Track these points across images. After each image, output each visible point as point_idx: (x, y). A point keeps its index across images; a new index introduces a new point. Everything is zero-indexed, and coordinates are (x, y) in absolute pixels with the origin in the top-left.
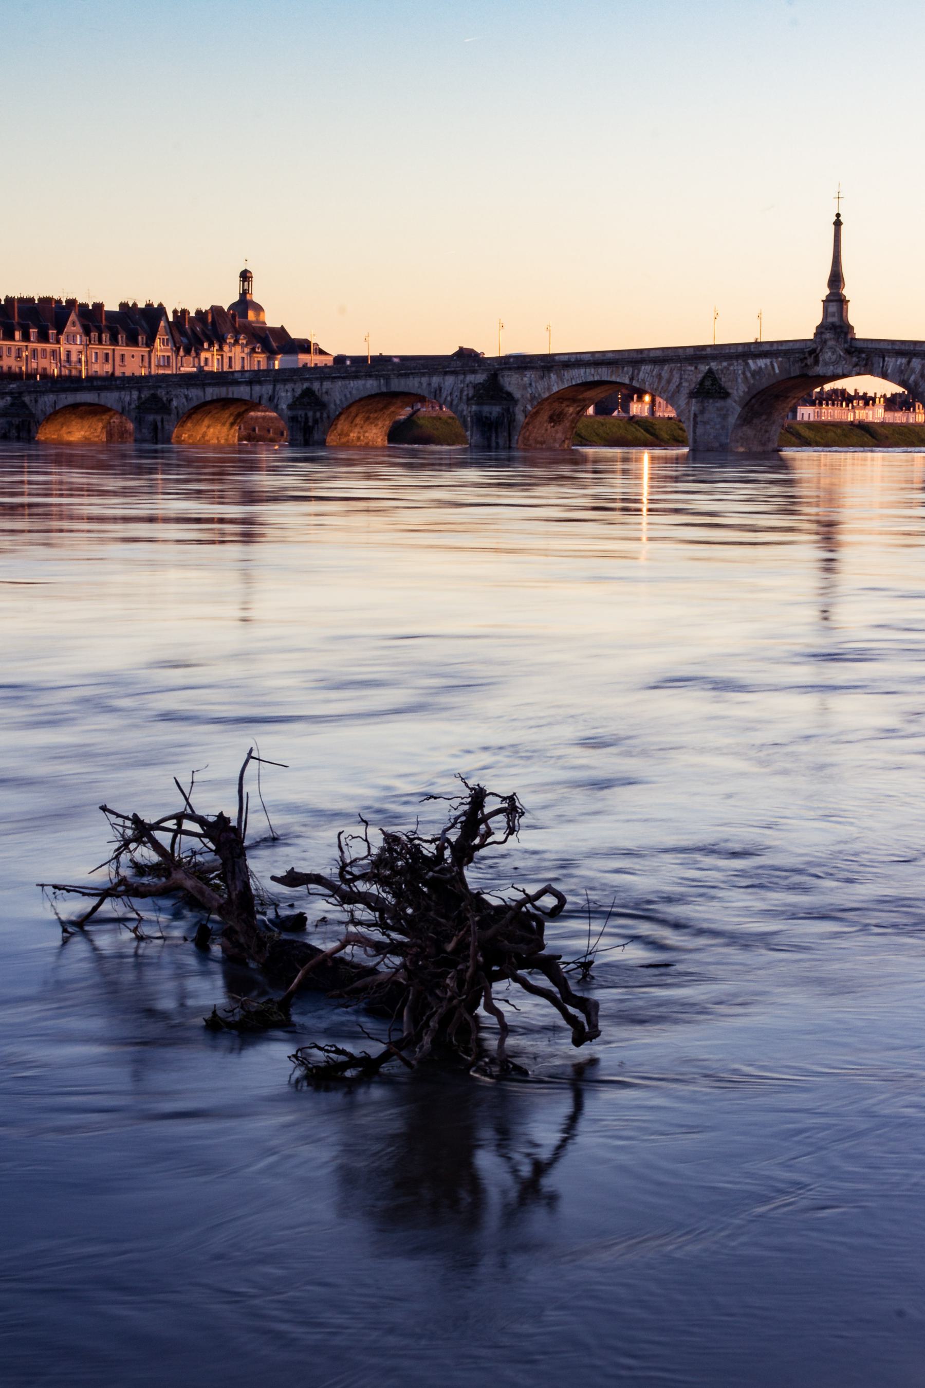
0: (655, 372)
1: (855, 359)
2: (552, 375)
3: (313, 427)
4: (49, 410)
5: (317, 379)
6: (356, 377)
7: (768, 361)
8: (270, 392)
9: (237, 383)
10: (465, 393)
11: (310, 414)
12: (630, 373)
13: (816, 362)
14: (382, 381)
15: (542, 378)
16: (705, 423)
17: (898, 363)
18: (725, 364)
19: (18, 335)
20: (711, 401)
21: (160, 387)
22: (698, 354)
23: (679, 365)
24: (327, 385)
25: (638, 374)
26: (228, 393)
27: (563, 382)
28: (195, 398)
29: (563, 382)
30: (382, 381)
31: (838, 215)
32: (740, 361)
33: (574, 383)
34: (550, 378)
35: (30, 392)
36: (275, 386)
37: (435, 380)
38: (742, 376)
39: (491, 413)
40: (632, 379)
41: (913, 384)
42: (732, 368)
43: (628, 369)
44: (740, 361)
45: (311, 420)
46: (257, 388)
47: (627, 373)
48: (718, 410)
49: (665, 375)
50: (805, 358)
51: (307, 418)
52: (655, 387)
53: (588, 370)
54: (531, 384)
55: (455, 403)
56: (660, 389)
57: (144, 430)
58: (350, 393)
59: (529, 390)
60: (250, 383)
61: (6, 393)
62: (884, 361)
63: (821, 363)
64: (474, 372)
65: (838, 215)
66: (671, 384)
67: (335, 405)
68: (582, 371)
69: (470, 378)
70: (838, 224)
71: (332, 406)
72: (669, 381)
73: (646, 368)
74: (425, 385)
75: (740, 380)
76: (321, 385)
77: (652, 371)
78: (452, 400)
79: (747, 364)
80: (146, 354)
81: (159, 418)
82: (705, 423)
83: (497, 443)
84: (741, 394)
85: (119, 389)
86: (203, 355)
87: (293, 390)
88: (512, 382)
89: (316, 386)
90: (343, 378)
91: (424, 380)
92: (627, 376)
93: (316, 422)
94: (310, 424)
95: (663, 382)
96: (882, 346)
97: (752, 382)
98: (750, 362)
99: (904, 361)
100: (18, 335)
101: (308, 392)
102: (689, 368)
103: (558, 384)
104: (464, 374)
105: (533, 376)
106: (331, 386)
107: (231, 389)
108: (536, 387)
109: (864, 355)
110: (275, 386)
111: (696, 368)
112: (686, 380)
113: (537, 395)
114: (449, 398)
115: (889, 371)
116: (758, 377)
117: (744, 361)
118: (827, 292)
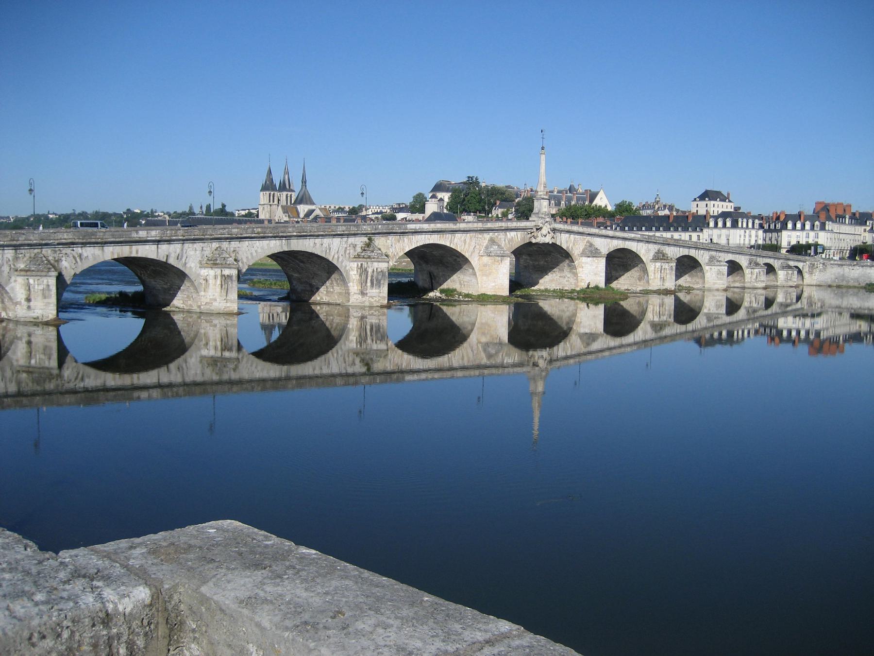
0: (462, 239)
2: (405, 239)
7: (516, 233)
8: (178, 251)
14: (284, 241)
18: (496, 234)
26: (131, 252)
27: (412, 244)
28: (90, 257)
34: (404, 241)
37: (326, 241)
43: (449, 236)
46: (164, 247)
49: (468, 241)
54: (392, 245)
66: (471, 247)
68: (423, 236)
72: (470, 245)
73: (458, 235)
74: (318, 245)
78: (338, 258)
79: (506, 235)
95: (467, 246)
99: (567, 235)
106: (239, 245)
107: (134, 248)
113: (395, 254)
114: (336, 256)
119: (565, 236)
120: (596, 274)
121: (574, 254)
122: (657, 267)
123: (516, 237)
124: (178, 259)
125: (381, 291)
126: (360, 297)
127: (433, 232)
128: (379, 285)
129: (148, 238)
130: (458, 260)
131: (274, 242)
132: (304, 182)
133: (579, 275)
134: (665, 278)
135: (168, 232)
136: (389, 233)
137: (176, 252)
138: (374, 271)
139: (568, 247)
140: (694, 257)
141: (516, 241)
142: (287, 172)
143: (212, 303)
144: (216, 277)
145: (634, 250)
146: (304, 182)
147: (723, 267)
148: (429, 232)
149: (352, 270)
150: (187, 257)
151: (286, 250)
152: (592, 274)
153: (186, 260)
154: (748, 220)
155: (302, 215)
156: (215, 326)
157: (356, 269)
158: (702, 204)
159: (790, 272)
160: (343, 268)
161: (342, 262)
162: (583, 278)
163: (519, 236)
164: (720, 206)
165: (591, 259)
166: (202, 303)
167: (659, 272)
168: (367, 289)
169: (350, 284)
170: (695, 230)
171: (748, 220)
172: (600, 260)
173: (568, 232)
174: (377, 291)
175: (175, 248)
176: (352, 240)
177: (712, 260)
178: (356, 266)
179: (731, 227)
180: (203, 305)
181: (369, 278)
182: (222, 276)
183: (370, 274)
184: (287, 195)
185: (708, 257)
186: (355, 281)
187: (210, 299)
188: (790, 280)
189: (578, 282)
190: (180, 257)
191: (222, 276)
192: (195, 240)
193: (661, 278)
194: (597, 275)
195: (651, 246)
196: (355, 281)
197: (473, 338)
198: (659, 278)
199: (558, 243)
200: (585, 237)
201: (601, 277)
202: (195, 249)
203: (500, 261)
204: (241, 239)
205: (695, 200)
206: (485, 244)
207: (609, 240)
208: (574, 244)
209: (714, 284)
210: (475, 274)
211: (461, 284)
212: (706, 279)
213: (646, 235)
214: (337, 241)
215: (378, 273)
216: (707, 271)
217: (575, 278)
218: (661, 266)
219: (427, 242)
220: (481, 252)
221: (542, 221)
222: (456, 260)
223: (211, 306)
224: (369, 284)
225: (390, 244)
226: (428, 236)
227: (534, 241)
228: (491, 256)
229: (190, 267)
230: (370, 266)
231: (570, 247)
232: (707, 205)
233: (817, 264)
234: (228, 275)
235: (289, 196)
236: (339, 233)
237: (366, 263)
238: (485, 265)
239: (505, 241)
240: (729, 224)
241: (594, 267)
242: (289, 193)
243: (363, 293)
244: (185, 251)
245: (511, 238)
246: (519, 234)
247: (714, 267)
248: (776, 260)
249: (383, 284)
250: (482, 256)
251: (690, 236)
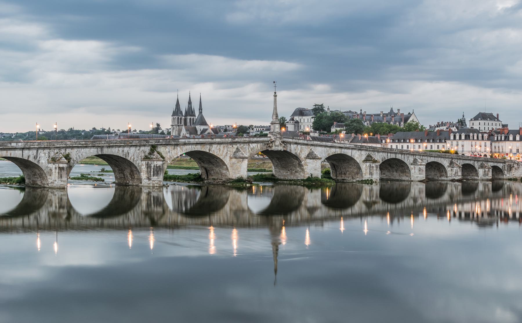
0: (218, 148)
6: (86, 147)
7: (256, 144)
8: (35, 154)
12: (209, 148)
14: (99, 149)
17: (294, 146)
18: (242, 145)
23: (226, 145)
24: (68, 151)
27: (183, 151)
29: (183, 151)
30: (99, 149)
32: (247, 144)
33: (187, 152)
34: (177, 149)
36: (37, 150)
37: (126, 149)
38: (248, 150)
40: (210, 150)
41: (298, 154)
42: (244, 147)
43: (208, 146)
44: (247, 144)
46: (26, 153)
50: (269, 144)
52: (218, 153)
53: (193, 146)
55: (135, 160)
56: (220, 154)
59: (168, 154)
62: (290, 145)
66: (224, 153)
68: (190, 146)
72: (223, 151)
73: (214, 146)
74: (121, 151)
75: (247, 151)
76: (66, 151)
78: (134, 158)
87: (49, 152)
90: (78, 147)
91: (121, 149)
92: (208, 149)
95: (221, 152)
98: (250, 144)
99: (296, 146)
103: (180, 152)
105: (170, 148)
107: (9, 152)
108: (171, 153)
110: (37, 150)
111: (232, 146)
113: (172, 156)
114: (132, 158)
115: (292, 149)
116: (253, 151)
117: (248, 144)
119: (293, 147)
120: (315, 170)
121: (301, 157)
122: (368, 165)
123: (257, 147)
124: (34, 158)
125: (159, 178)
126: (148, 181)
127: (197, 144)
128: (157, 174)
129: (17, 147)
130: (218, 160)
131: (93, 149)
132: (201, 109)
133: (305, 170)
134: (373, 173)
135: (29, 144)
136: (167, 145)
137: (33, 155)
138: (154, 166)
139: (296, 153)
140: (401, 159)
141: (256, 149)
142: (190, 103)
143: (54, 183)
144: (56, 168)
145: (350, 154)
146: (201, 109)
147: (423, 166)
148: (194, 144)
149: (143, 165)
150: (40, 157)
151: (101, 154)
152: (313, 169)
153: (39, 159)
154: (473, 134)
155: (199, 133)
156: (56, 195)
157: (145, 165)
158: (476, 123)
159: (487, 170)
160: (137, 164)
161: (136, 161)
162: (308, 172)
163: (259, 146)
164: (490, 124)
165: (312, 160)
166: (49, 182)
167: (369, 168)
168: (151, 177)
169: (142, 174)
170: (440, 141)
171: (473, 134)
172: (318, 161)
173: (296, 143)
174: (157, 177)
175: (32, 153)
176: (142, 148)
177: (415, 162)
178: (145, 163)
179: (454, 140)
180: (49, 183)
181: (152, 170)
182: (59, 168)
183: (152, 167)
184: (190, 118)
185: (413, 160)
186: (145, 172)
187: (53, 180)
188: (487, 175)
189: (305, 175)
190: (35, 157)
191: (59, 168)
192: (44, 148)
193: (370, 173)
194: (316, 171)
195: (363, 152)
196: (145, 172)
197: (227, 207)
198: (369, 172)
199: (288, 150)
200: (309, 147)
201: (319, 171)
202: (45, 153)
203: (242, 161)
204: (72, 148)
205: (471, 120)
206: (234, 151)
207: (328, 149)
208: (301, 151)
209: (417, 177)
210: (227, 169)
211: (221, 175)
212: (412, 174)
213: (359, 145)
214: (133, 149)
215: (156, 166)
216: (412, 168)
217: (303, 172)
218: (370, 165)
219: (193, 150)
220: (231, 156)
221: (274, 137)
222: (216, 160)
223: (53, 184)
224: (152, 174)
225: (168, 151)
226: (194, 146)
227: (270, 149)
228: (237, 158)
229: (42, 163)
230: (153, 163)
231: (298, 153)
232: (480, 123)
233: (513, 165)
234: (62, 167)
235: (192, 119)
236: (133, 144)
237: (150, 162)
238: (234, 163)
239: (248, 149)
240: (463, 137)
241: (314, 165)
242: (192, 118)
243: (149, 179)
244: (38, 154)
245: (253, 147)
246: (259, 145)
247: (416, 166)
248: (476, 162)
249: (160, 174)
250: (232, 158)
251: (402, 146)
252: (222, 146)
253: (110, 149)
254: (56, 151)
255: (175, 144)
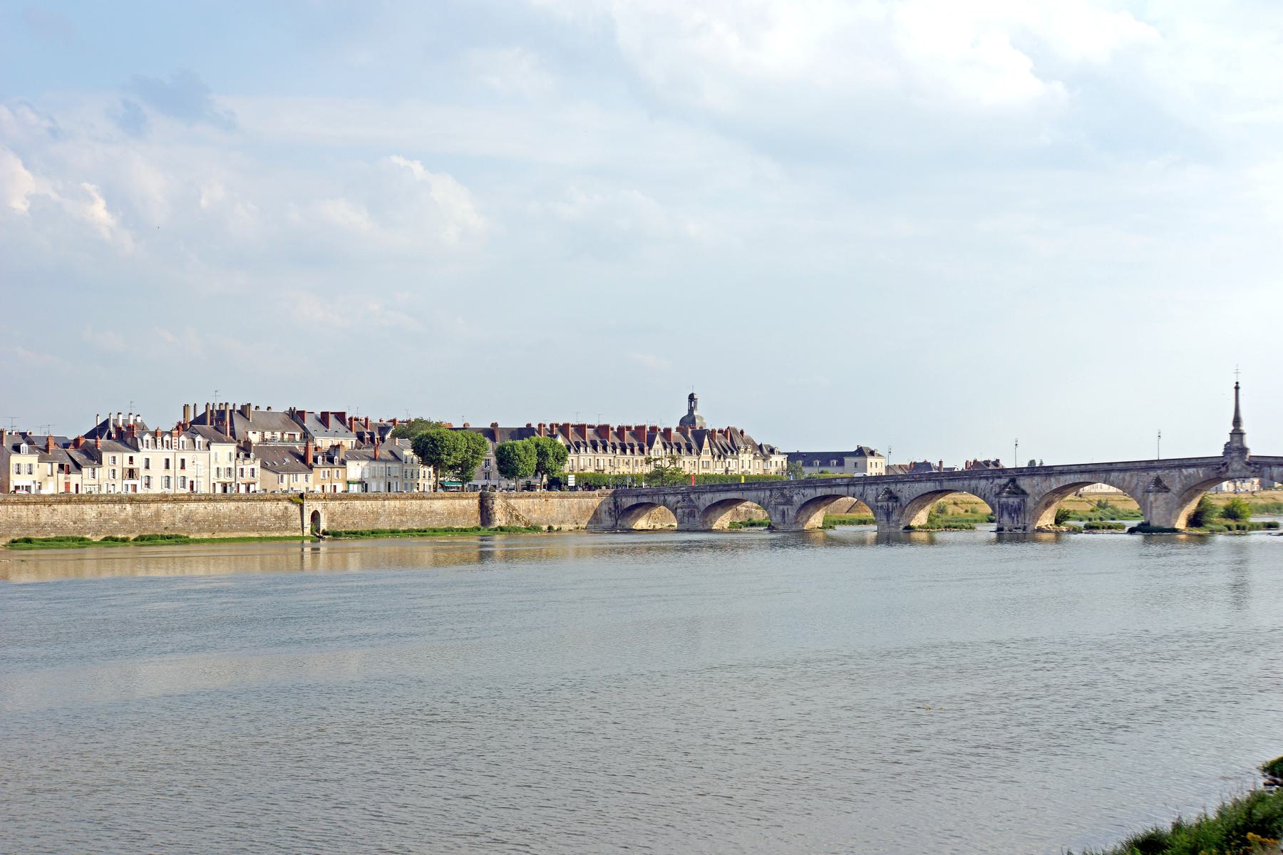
0: (1120, 477)
1: (1253, 468)
3: (892, 512)
4: (708, 504)
5: (893, 482)
6: (920, 481)
7: (1195, 469)
8: (861, 490)
9: (839, 485)
10: (994, 490)
11: (890, 504)
13: (1227, 470)
15: (1045, 481)
16: (1157, 507)
18: (1167, 471)
19: (628, 451)
20: (1160, 494)
21: (786, 488)
22: (1149, 466)
24: (900, 486)
25: (1109, 478)
31: (1237, 383)
34: (1050, 481)
35: (695, 493)
36: (864, 487)
39: (1014, 503)
42: (1171, 474)
45: (891, 508)
47: (1102, 477)
48: (1165, 499)
51: (888, 506)
57: (777, 516)
58: (916, 490)
60: (848, 485)
61: (678, 493)
63: (1230, 471)
64: (1000, 477)
65: (1237, 383)
67: (905, 498)
68: (1072, 476)
69: (997, 481)
70: (1237, 388)
71: (904, 499)
74: (966, 485)
77: (1119, 476)
78: (985, 495)
79: (1181, 471)
80: (697, 460)
81: (785, 507)
82: (1157, 507)
83: (1018, 521)
84: (1178, 489)
85: (756, 489)
86: (727, 460)
87: (877, 489)
88: (1024, 483)
89: (892, 487)
93: (893, 509)
94: (890, 510)
96: (1269, 460)
97: (1185, 482)
98: (1183, 470)
100: (628, 451)
101: (889, 492)
102: (1144, 474)
104: (993, 478)
107: (834, 489)
109: (1258, 466)
110: (864, 487)
112: (1142, 481)
118: (1232, 428)
136: (1034, 475)
252: (1128, 474)
253: (951, 483)
254: (885, 486)
255: (1046, 474)
